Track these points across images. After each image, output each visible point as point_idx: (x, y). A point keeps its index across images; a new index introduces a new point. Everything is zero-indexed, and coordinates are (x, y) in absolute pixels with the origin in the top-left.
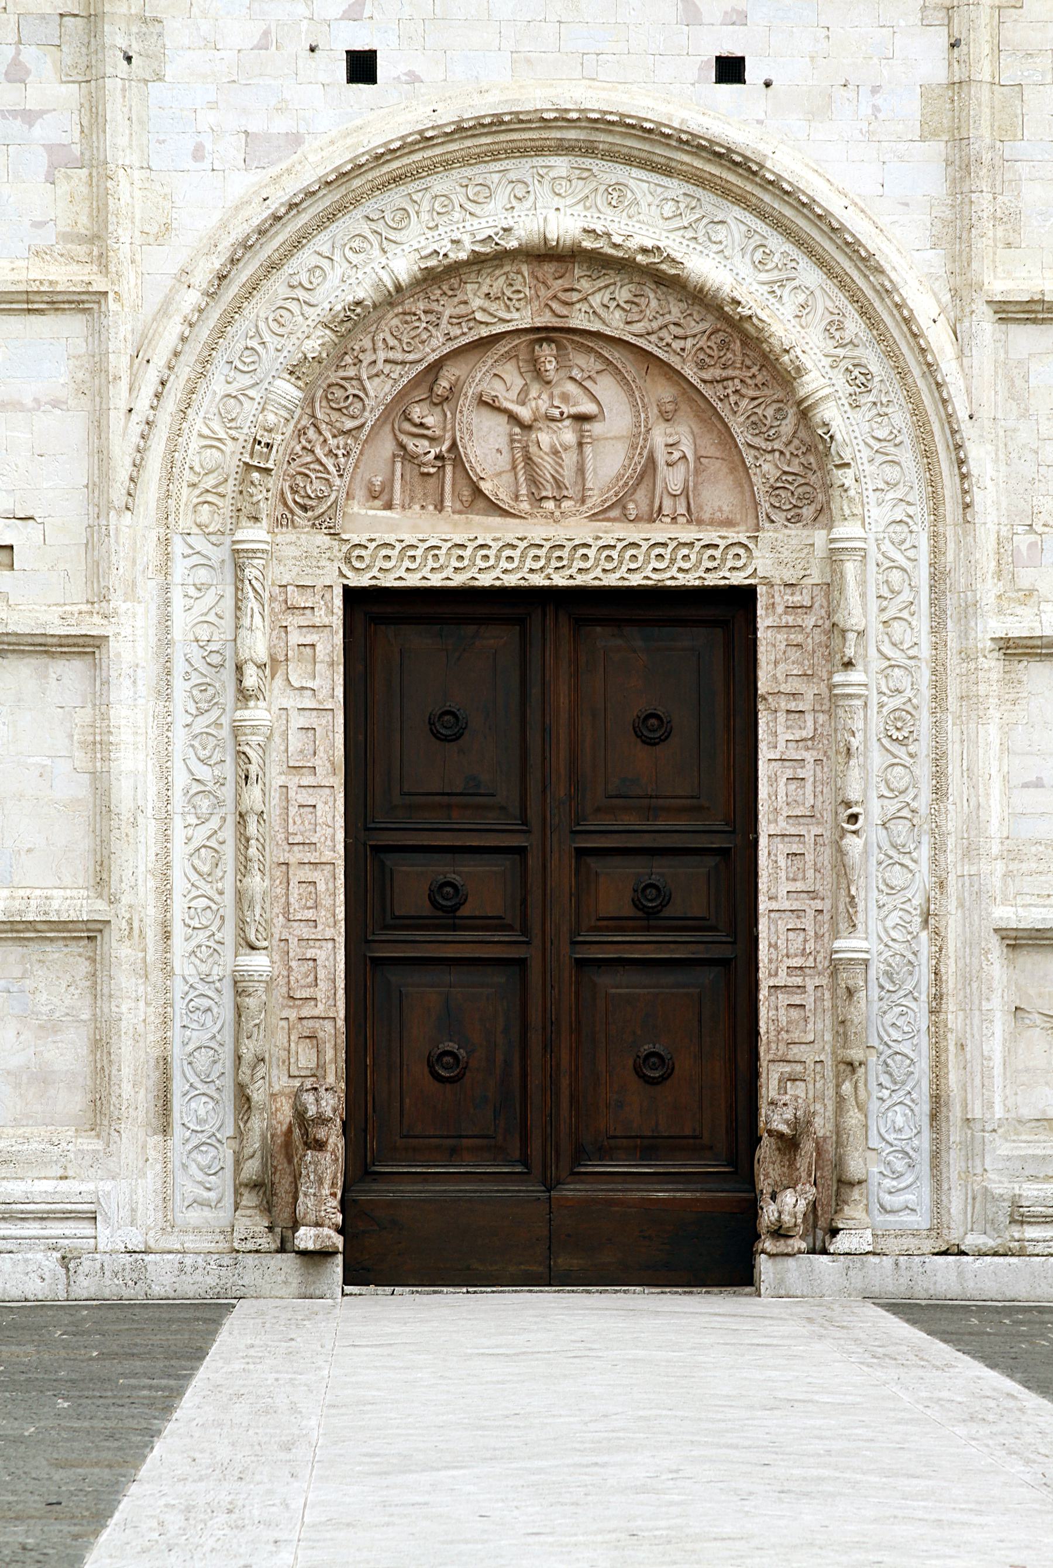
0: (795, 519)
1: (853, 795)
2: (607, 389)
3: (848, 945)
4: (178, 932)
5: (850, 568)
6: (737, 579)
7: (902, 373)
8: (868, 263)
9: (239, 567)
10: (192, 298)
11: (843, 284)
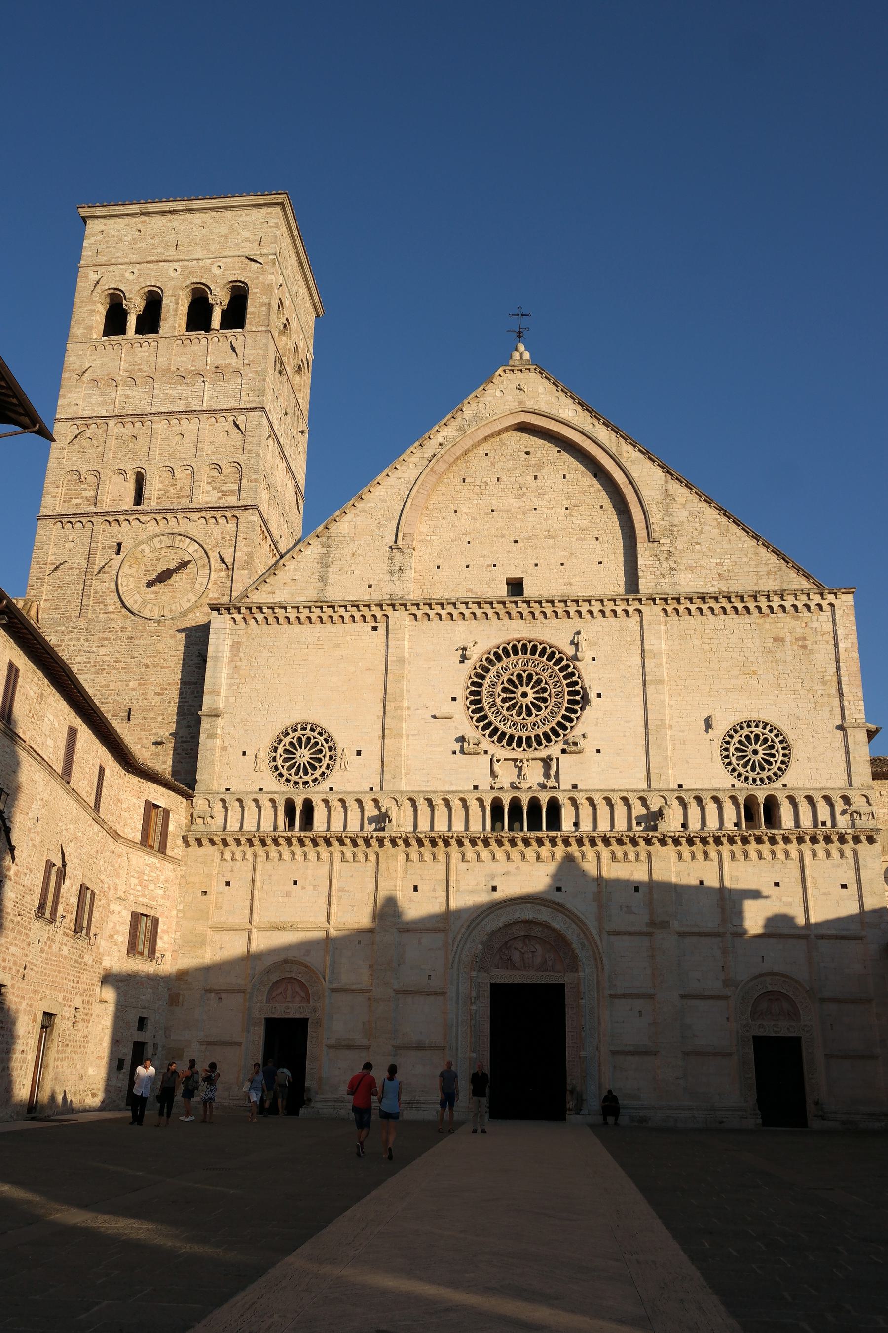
0: (572, 971)
1: (583, 1024)
2: (537, 946)
3: (583, 1053)
4: (459, 1048)
5: (582, 981)
6: (561, 982)
7: (591, 944)
8: (584, 924)
9: (471, 979)
10: (463, 930)
11: (580, 928)
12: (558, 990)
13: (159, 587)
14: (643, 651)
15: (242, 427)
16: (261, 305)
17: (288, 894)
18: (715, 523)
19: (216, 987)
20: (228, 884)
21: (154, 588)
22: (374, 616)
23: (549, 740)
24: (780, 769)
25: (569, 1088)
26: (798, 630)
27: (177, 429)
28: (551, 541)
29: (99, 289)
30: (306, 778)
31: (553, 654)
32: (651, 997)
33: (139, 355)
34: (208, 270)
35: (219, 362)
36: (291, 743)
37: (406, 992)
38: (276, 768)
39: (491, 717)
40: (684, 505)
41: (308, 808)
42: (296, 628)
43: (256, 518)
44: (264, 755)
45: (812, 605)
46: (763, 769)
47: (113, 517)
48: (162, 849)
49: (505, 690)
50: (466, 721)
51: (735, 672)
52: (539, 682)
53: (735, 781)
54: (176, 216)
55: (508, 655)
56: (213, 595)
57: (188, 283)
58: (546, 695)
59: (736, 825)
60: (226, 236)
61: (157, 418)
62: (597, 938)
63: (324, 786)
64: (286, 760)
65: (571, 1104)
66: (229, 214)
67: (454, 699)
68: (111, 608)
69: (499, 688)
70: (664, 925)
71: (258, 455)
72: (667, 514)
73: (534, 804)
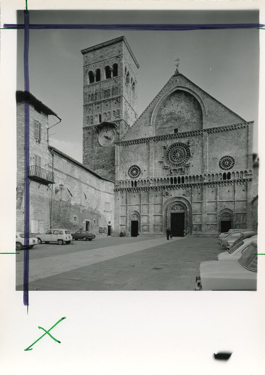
24: (232, 166)
30: (135, 176)
33: (97, 87)
38: (129, 175)
59: (221, 179)
62: (191, 204)
63: (138, 178)
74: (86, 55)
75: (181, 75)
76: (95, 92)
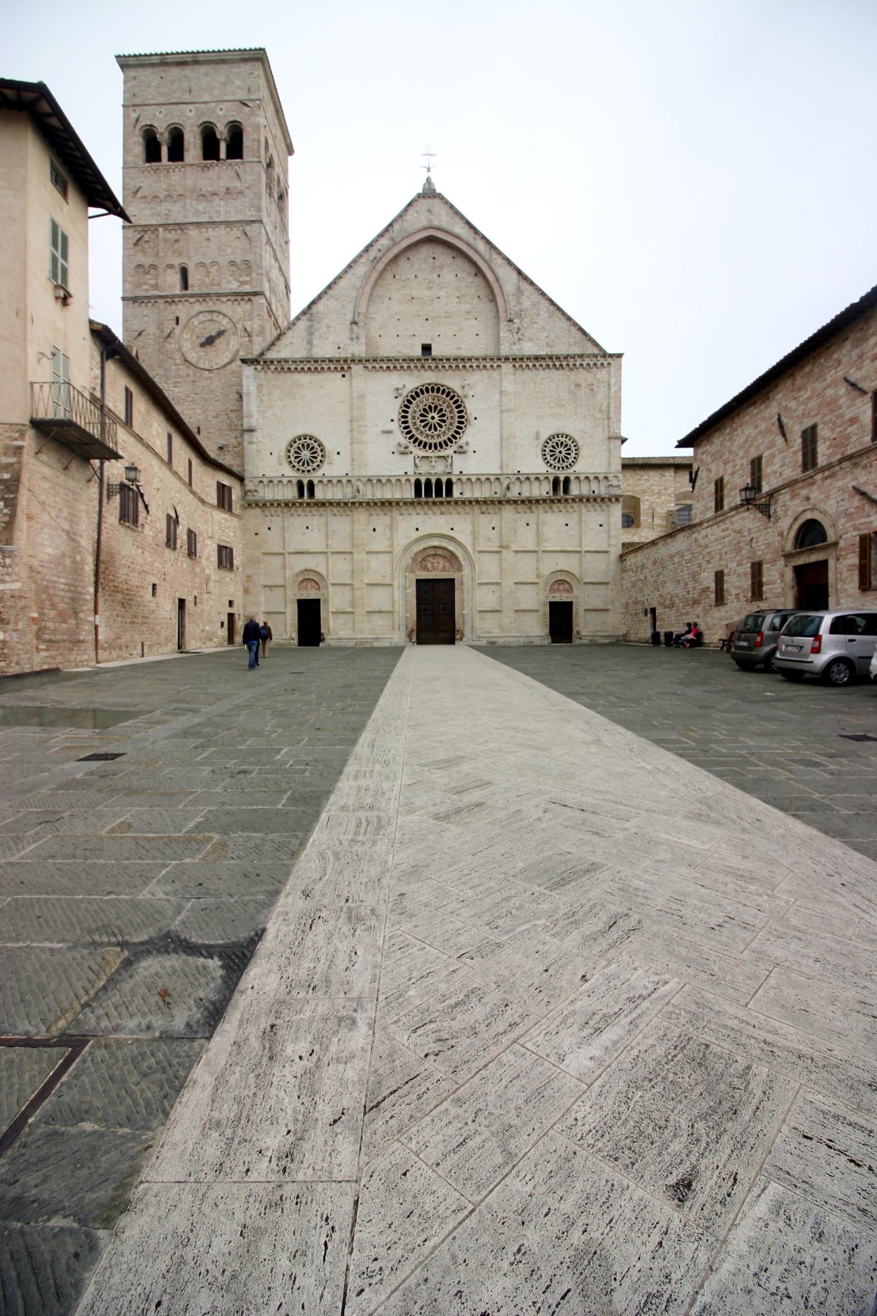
12: (452, 581)
13: (208, 348)
14: (501, 392)
15: (249, 235)
16: (254, 141)
17: (304, 534)
18: (546, 310)
19: (268, 584)
20: (269, 529)
21: (205, 349)
22: (342, 368)
23: (447, 445)
25: (457, 628)
26: (589, 379)
27: (205, 235)
28: (448, 320)
29: (139, 126)
30: (309, 468)
31: (449, 393)
32: (499, 584)
33: (174, 178)
34: (214, 111)
35: (229, 185)
36: (298, 448)
37: (372, 585)
38: (291, 462)
39: (414, 432)
40: (528, 297)
41: (311, 485)
42: (296, 376)
43: (263, 301)
44: (283, 454)
45: (599, 364)
46: (564, 461)
47: (171, 300)
48: (230, 510)
49: (422, 415)
50: (400, 434)
51: (552, 405)
52: (441, 410)
53: (549, 469)
54: (187, 67)
55: (423, 393)
56: (242, 354)
57: (201, 121)
58: (445, 418)
60: (224, 84)
61: (191, 227)
63: (320, 473)
64: (296, 458)
65: (458, 637)
66: (225, 67)
67: (392, 420)
68: (178, 362)
69: (418, 414)
70: (507, 547)
71: (261, 255)
72: (519, 302)
73: (439, 482)
74: (132, 73)
75: (440, 197)
76: (166, 193)
